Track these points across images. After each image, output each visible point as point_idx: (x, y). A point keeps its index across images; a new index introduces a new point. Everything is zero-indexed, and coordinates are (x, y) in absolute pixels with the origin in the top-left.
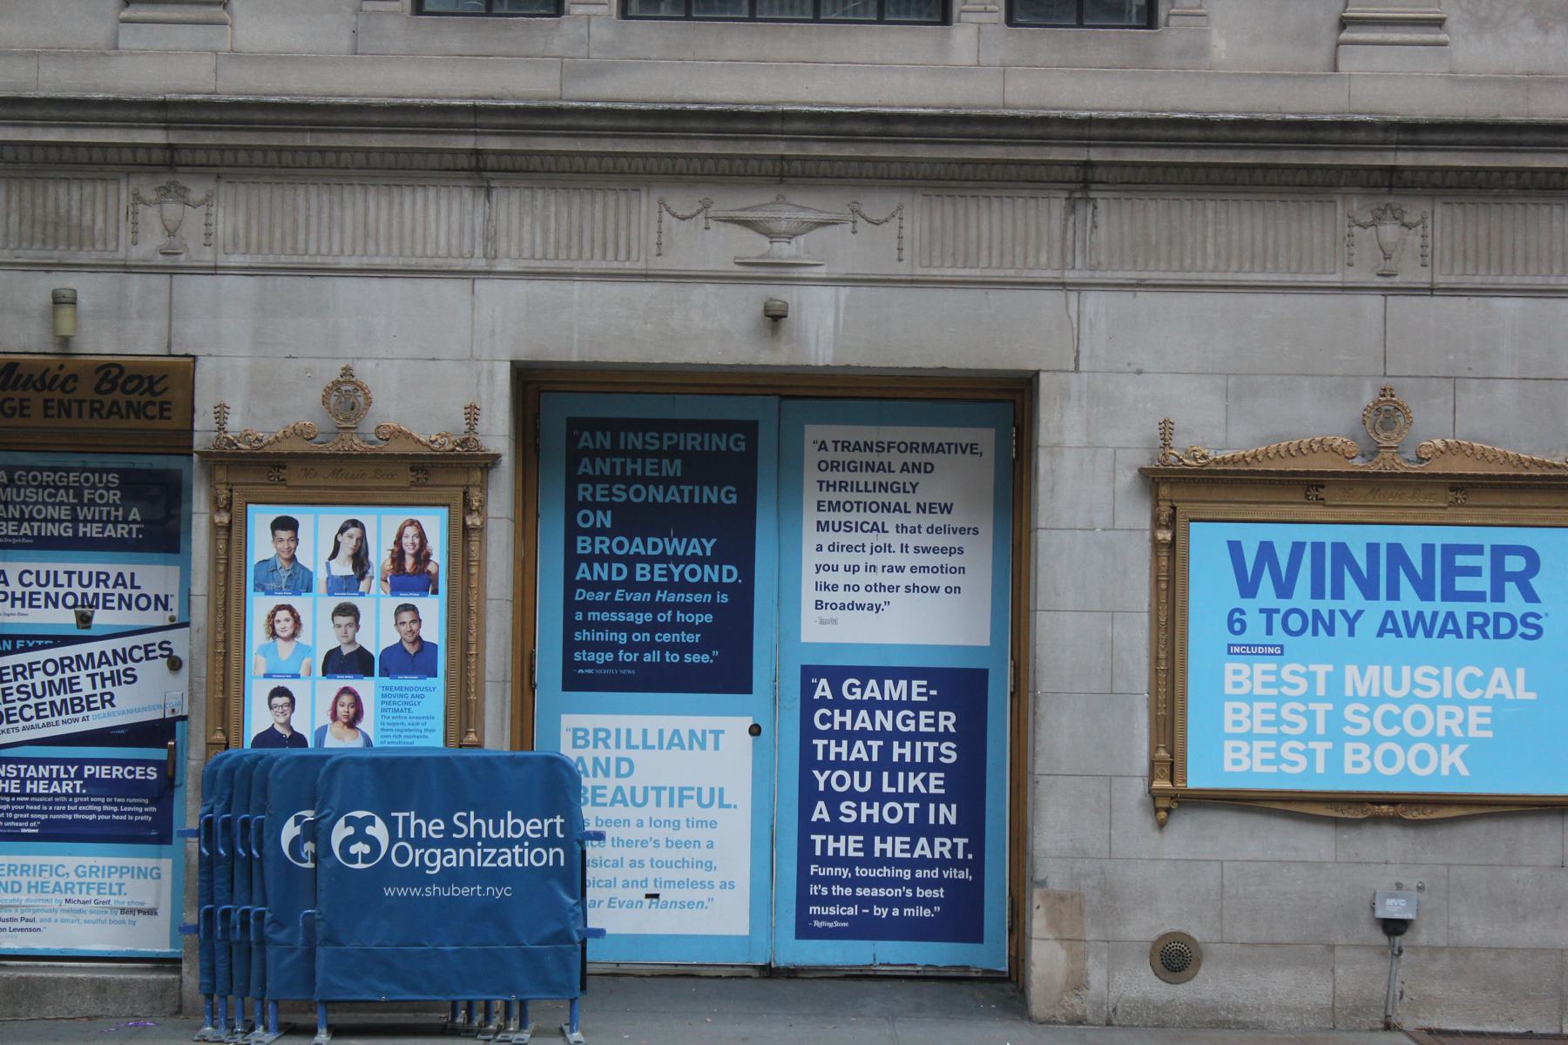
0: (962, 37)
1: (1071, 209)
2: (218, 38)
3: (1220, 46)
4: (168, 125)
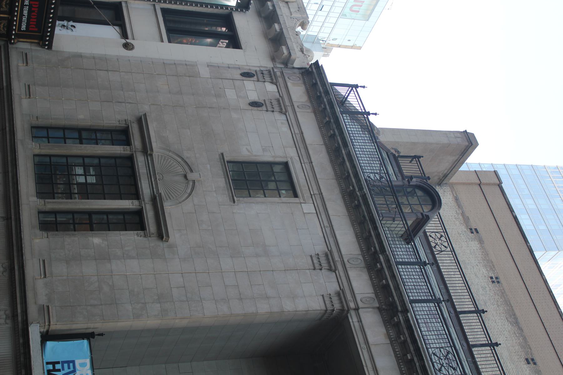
0: (35, 199)
1: (2, 217)
2: (23, 96)
3: (37, 241)
4: (7, 86)
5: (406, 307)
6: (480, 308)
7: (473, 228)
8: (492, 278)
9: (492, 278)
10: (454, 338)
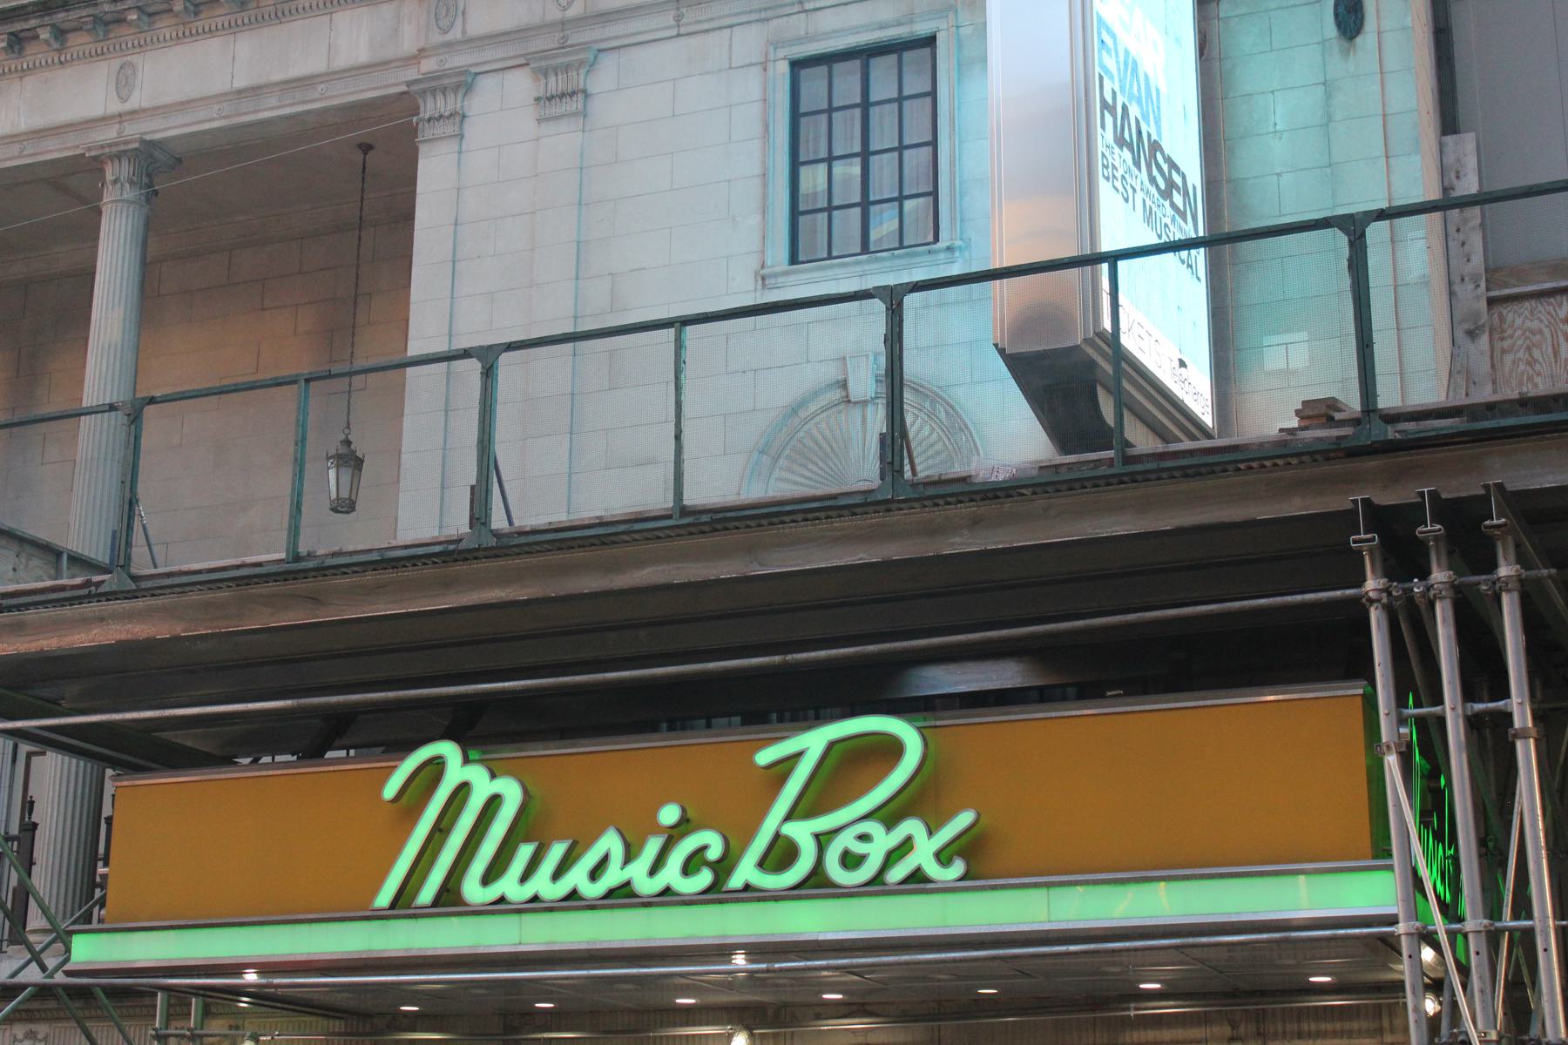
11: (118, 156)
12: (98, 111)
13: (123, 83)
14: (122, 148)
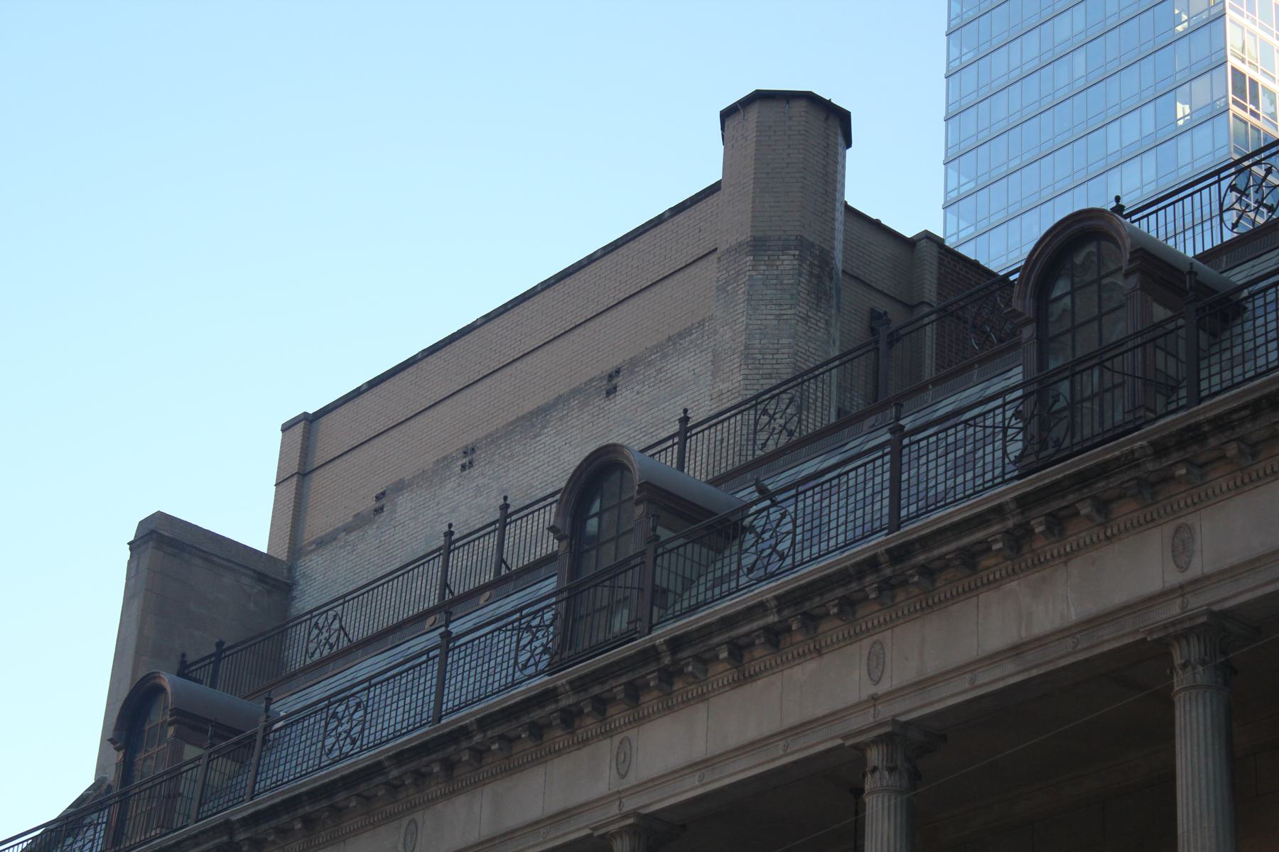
5: (221, 824)
6: (441, 542)
7: (371, 503)
8: (463, 467)
9: (463, 467)
10: (469, 625)
11: (1185, 635)
12: (1155, 586)
13: (1181, 550)
14: (1187, 625)
